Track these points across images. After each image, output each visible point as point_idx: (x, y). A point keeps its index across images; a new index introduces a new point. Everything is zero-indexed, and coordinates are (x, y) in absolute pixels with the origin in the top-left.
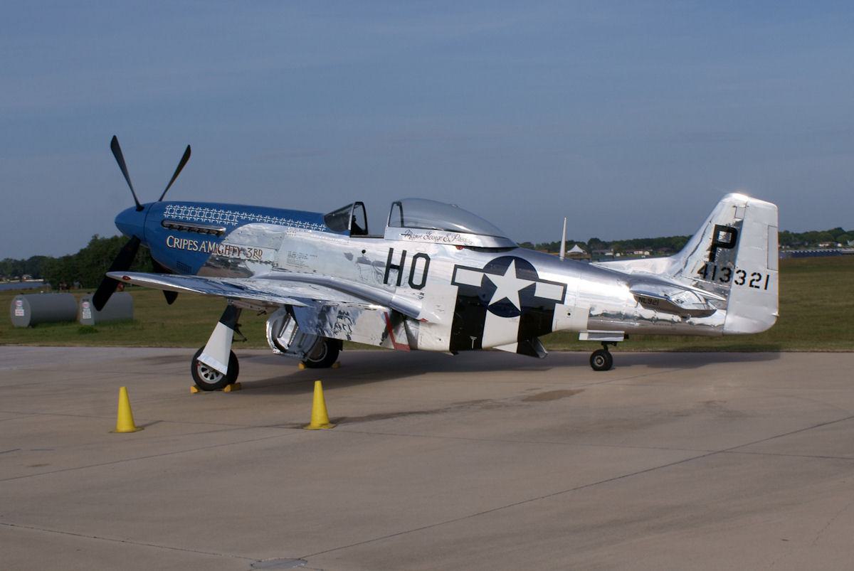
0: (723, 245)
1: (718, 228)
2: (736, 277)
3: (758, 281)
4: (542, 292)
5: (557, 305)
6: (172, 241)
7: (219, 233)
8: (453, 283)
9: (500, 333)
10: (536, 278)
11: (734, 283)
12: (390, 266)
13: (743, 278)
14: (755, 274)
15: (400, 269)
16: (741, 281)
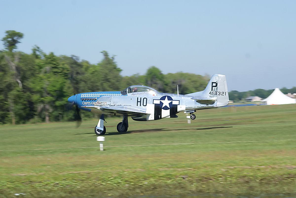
0: (214, 86)
1: (213, 83)
2: (218, 93)
3: (223, 94)
4: (174, 103)
5: (178, 105)
6: (84, 103)
7: (96, 99)
8: (153, 104)
9: (165, 113)
10: (172, 100)
11: (218, 95)
12: (138, 102)
13: (220, 93)
14: (222, 92)
15: (140, 102)
16: (219, 94)
